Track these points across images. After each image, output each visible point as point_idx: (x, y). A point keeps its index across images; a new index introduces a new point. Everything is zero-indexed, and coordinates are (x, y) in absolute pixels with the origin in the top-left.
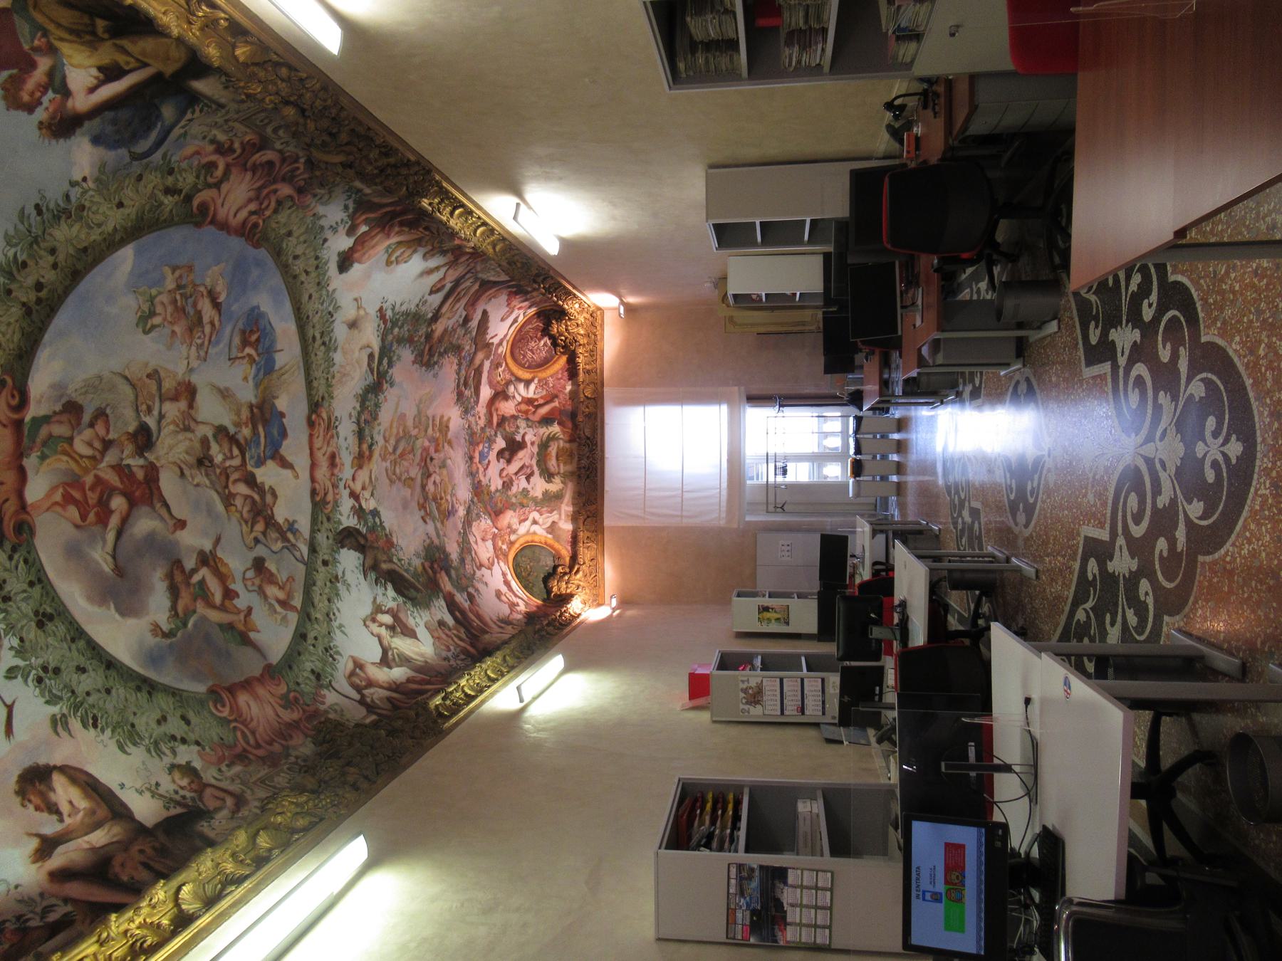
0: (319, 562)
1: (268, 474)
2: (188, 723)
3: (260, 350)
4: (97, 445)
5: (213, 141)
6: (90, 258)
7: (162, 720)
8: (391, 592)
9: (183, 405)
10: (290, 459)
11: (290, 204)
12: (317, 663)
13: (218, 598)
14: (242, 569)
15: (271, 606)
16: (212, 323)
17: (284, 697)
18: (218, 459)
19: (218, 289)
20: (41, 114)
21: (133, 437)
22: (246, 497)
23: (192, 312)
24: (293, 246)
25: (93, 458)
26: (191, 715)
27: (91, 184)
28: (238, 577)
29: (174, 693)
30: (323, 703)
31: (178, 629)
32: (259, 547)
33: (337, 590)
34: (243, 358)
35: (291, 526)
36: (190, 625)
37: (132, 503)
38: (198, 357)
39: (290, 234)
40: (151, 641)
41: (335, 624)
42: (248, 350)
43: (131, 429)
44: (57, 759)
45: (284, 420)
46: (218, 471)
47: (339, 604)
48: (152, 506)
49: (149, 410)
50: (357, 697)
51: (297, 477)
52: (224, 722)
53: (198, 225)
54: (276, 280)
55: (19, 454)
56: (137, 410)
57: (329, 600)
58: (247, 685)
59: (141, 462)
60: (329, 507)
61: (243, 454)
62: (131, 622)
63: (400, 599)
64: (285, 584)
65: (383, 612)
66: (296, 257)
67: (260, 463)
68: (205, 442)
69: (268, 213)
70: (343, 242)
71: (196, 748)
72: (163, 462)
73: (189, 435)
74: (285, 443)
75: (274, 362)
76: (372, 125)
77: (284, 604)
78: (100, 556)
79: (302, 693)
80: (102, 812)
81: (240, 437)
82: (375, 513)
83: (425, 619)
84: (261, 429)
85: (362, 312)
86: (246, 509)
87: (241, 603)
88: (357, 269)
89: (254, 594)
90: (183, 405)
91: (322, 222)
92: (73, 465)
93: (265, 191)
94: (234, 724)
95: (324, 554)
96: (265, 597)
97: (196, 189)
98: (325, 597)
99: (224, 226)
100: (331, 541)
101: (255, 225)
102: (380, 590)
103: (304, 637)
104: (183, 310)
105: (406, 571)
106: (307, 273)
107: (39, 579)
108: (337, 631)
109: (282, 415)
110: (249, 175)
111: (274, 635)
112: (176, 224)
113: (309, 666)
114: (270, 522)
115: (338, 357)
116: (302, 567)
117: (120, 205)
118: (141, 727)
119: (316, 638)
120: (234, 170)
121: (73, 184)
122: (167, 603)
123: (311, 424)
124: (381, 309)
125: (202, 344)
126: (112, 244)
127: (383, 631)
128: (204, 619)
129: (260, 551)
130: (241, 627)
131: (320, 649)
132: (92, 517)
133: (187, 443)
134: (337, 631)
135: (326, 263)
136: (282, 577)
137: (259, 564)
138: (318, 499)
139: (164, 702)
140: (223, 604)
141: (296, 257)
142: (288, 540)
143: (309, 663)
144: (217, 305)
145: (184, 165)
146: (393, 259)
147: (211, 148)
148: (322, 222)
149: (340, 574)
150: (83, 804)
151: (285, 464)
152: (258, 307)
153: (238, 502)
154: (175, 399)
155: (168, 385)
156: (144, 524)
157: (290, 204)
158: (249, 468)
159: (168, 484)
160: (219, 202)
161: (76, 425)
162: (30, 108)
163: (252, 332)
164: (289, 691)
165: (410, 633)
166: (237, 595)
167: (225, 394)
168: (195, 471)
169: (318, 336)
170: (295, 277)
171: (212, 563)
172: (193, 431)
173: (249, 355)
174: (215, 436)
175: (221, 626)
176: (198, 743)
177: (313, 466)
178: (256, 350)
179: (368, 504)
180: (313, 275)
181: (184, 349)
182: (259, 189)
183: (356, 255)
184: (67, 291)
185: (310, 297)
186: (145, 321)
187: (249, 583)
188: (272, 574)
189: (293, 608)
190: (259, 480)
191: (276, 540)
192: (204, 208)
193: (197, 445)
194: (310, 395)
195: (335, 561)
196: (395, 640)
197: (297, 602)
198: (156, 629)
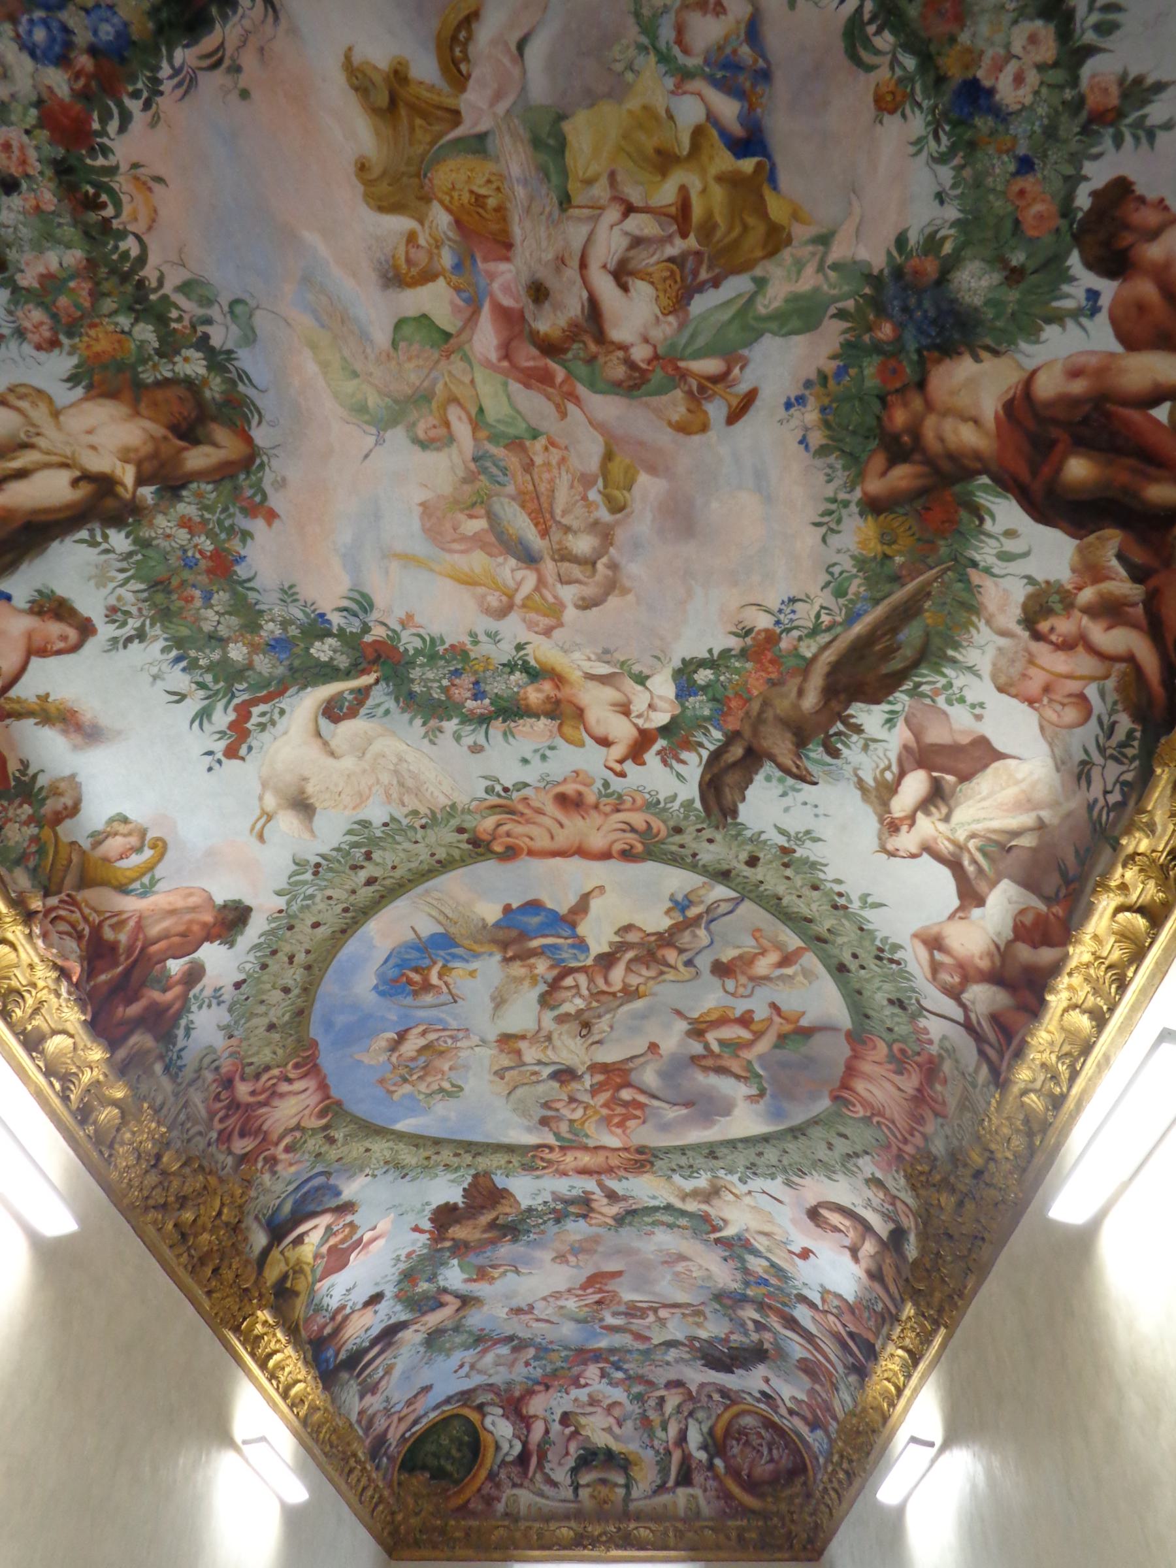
0: (748, 871)
1: (598, 934)
2: (845, 1136)
3: (427, 962)
4: (574, 1105)
5: (274, 1173)
6: (416, 1140)
7: (830, 1146)
8: (870, 717)
9: (523, 1045)
10: (572, 900)
11: (248, 1070)
12: (886, 986)
13: (745, 1034)
14: (721, 993)
15: (781, 978)
16: (424, 1033)
17: (891, 1058)
18: (580, 1003)
19: (384, 1044)
20: (349, 1218)
21: (562, 1082)
22: (628, 969)
23: (422, 1059)
24: (279, 1008)
25: (585, 1108)
26: (842, 1129)
27: (367, 1171)
28: (730, 1001)
29: (815, 1121)
30: (931, 1042)
31: (760, 1083)
32: (697, 961)
33: (805, 861)
34: (446, 984)
35: (680, 905)
36: (761, 1072)
37: (628, 1085)
38: (467, 1037)
39: (271, 1027)
40: (761, 1106)
41: (855, 906)
42: (434, 979)
43: (556, 1085)
44: (814, 1203)
45: (514, 906)
46: (594, 1004)
47: (830, 873)
48: (631, 1070)
49: (535, 1073)
50: (958, 1014)
51: (601, 889)
52: (867, 1120)
53: (339, 1103)
54: (329, 987)
55: (585, 1148)
56: (538, 1082)
57: (815, 888)
58: (851, 1071)
59: (587, 1077)
60: (656, 824)
61: (571, 971)
62: (737, 1112)
63: (901, 700)
64: (761, 946)
65: (892, 789)
66: (286, 990)
67: (581, 945)
68: (561, 1019)
69: (276, 1072)
70: (220, 962)
71: (867, 1158)
72: (587, 1059)
73: (555, 1036)
74: (550, 905)
75: (433, 936)
76: (189, 1281)
77: (787, 960)
78: (672, 1113)
79: (903, 1039)
80: (860, 1228)
81: (551, 975)
82: (684, 676)
83: (985, 668)
84: (535, 943)
85: (270, 802)
86: (644, 972)
87: (761, 1013)
88: (224, 889)
89: (758, 989)
90: (523, 1045)
91: (226, 1018)
92: (594, 1119)
93: (262, 1097)
94: (875, 1119)
95: (736, 858)
96: (767, 978)
97: (314, 1131)
98: (806, 891)
99: (323, 1086)
100: (718, 837)
101: (297, 1066)
102: (852, 753)
103: (842, 968)
104: (424, 1068)
105: (852, 618)
106: (291, 959)
107: (683, 1150)
108: (868, 914)
109: (507, 909)
110: (265, 1127)
111: (820, 999)
112: (351, 1114)
113: (881, 998)
114: (667, 939)
115: (377, 814)
116: (747, 907)
117: (367, 1150)
118: (825, 1159)
119: (855, 956)
120: (274, 1137)
121: (374, 1176)
122: (732, 1081)
123: (511, 853)
124: (231, 752)
125: (451, 1037)
126: (400, 1136)
127: (926, 826)
128: (760, 1057)
129: (704, 962)
130: (788, 1028)
131: (872, 964)
132: (638, 1113)
133: (564, 1037)
134: (868, 914)
135: (256, 947)
136: (749, 945)
137: (722, 970)
138: (639, 847)
139: (817, 1132)
140: (754, 1033)
141: (286, 990)
142: (699, 917)
143: (879, 996)
144: (402, 1037)
145: (306, 1156)
146: (148, 853)
147: (279, 1168)
148: (226, 1018)
149: (782, 841)
150: (847, 1223)
151: (582, 906)
152: (376, 987)
153: (634, 980)
154: (519, 1053)
155: (506, 1061)
156: (649, 1077)
157: (248, 1070)
158: (589, 962)
159: (609, 1055)
160: (307, 1112)
161: (559, 1119)
162: (351, 1224)
163: (410, 982)
164: (890, 1046)
165: (979, 755)
166: (751, 1012)
167: (499, 1002)
168: (595, 1029)
169: (363, 875)
170: (308, 968)
171: (703, 1026)
172: (550, 1033)
173: (440, 976)
174: (553, 1008)
175: (776, 1046)
176: (867, 1153)
177: (581, 852)
178: (429, 968)
179: (658, 700)
180: (287, 948)
181: (462, 1054)
182: (265, 1104)
183: (208, 918)
184: (454, 1141)
185: (316, 925)
186: (453, 1092)
187: (741, 990)
188: (740, 957)
189: (798, 952)
190: (606, 949)
191: (695, 936)
192: (322, 1114)
193: (566, 1027)
194: (463, 862)
195: (755, 839)
196: (959, 815)
197: (793, 941)
198: (750, 1098)
